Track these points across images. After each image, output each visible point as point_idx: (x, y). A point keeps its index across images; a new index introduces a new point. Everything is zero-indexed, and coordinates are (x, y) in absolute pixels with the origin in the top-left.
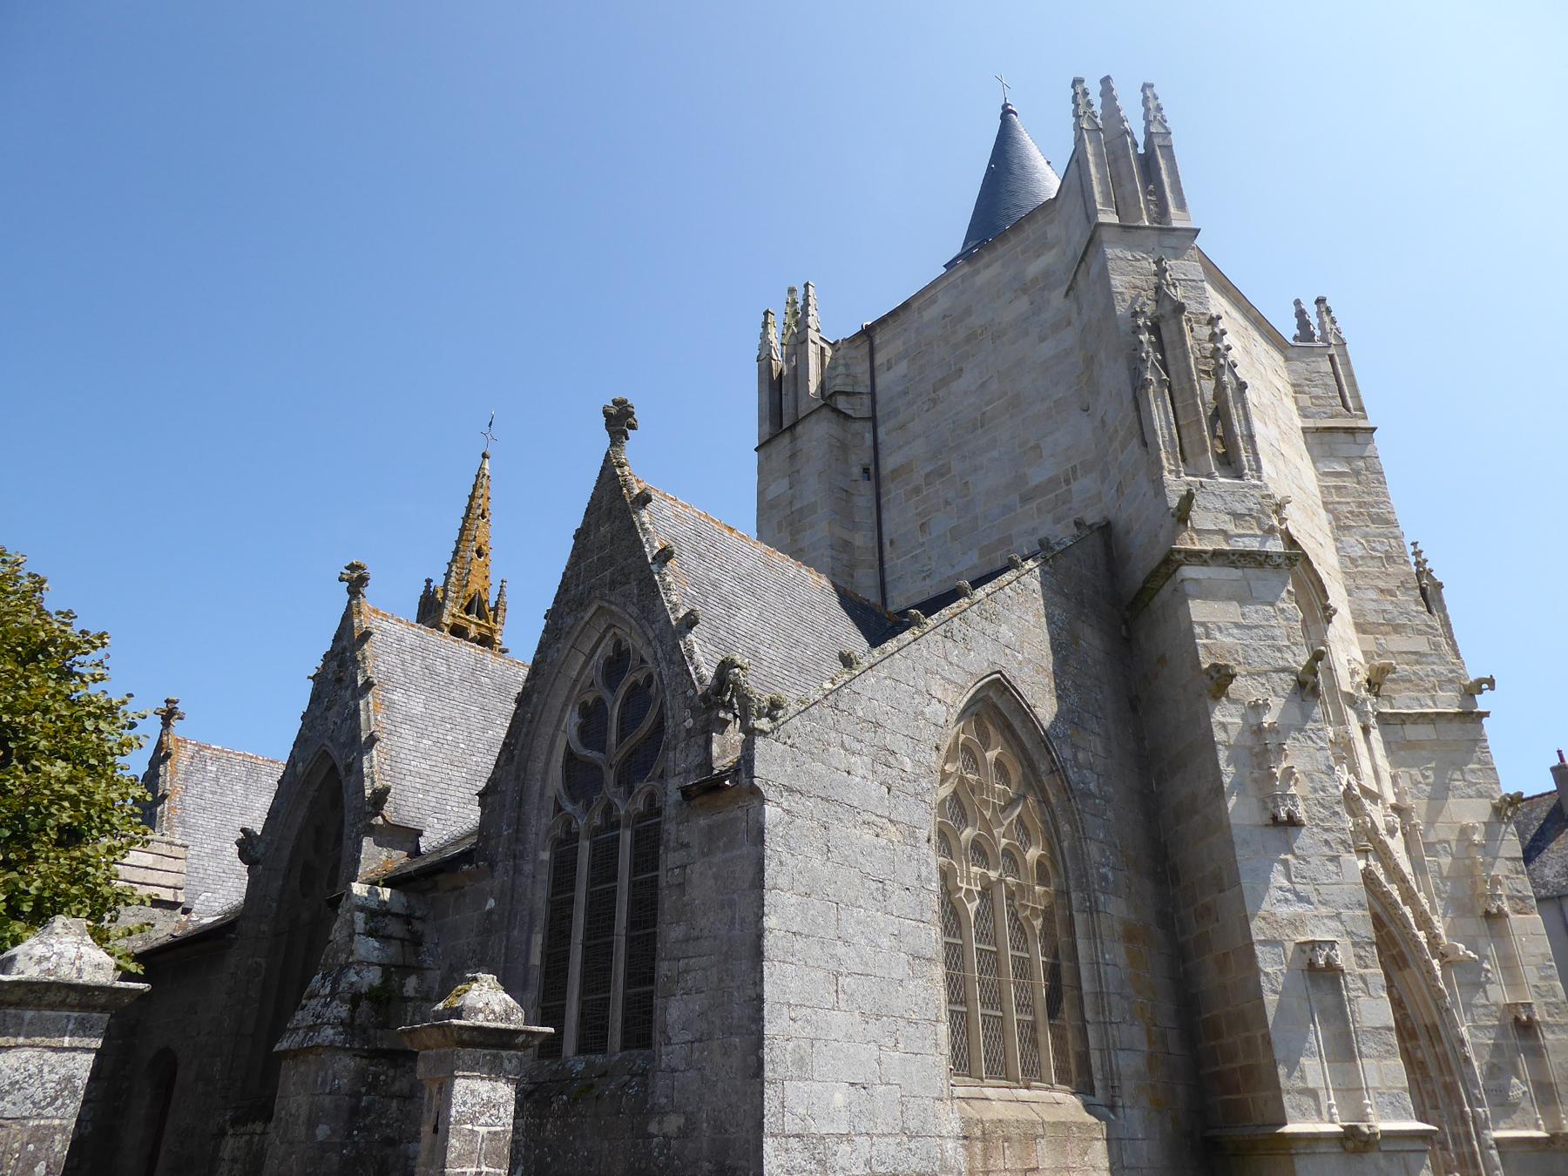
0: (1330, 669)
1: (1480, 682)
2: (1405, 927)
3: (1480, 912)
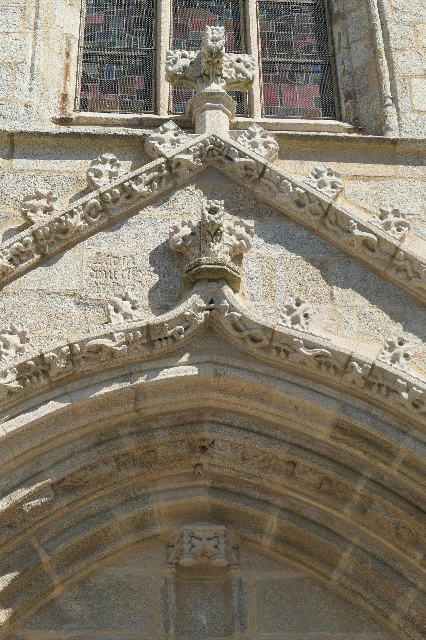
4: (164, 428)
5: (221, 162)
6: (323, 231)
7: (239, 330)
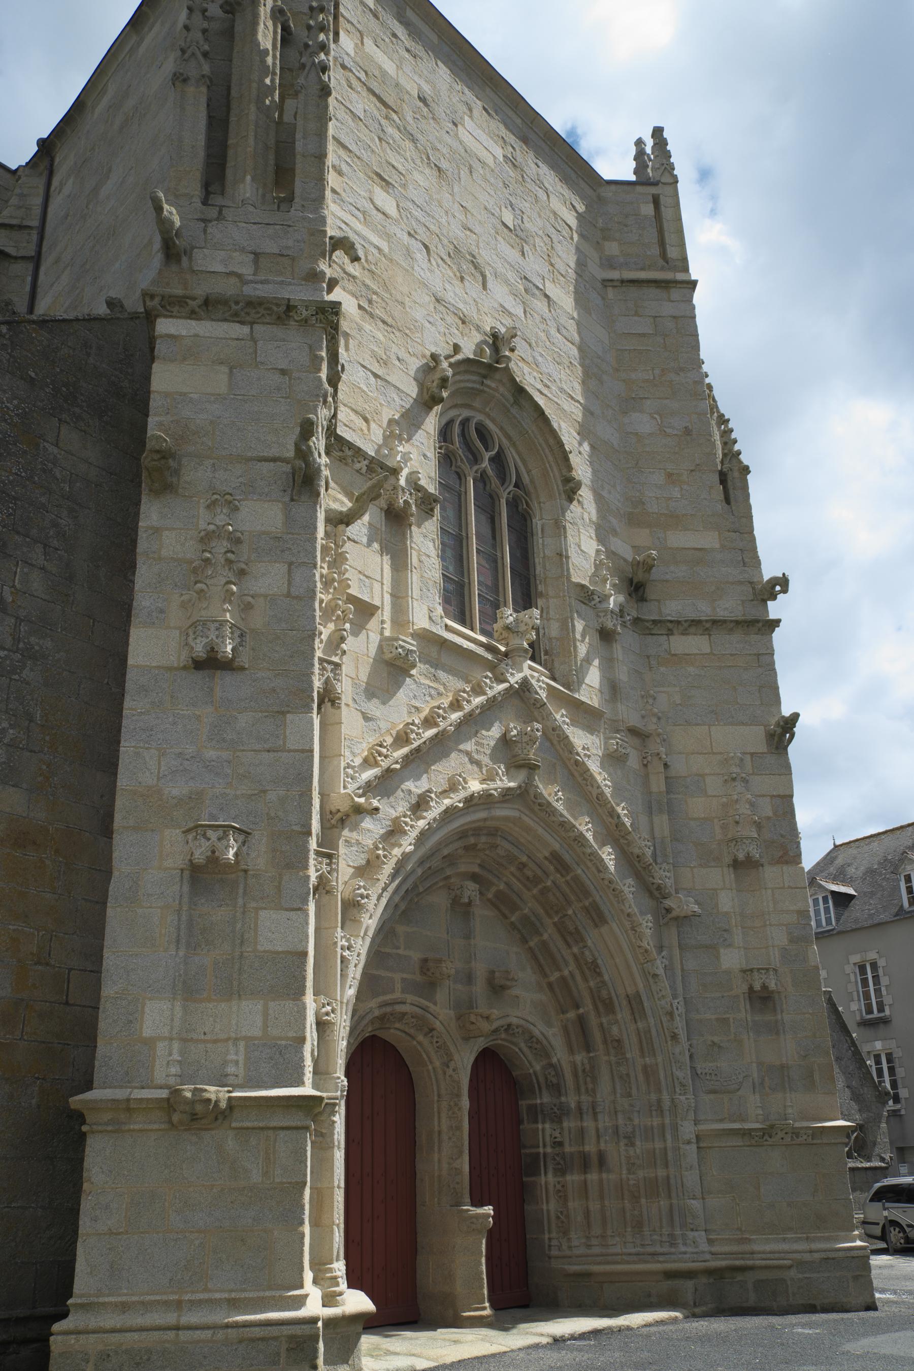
0: (561, 555)
1: (774, 581)
2: (599, 871)
3: (728, 860)
5: (524, 692)
6: (558, 747)
7: (536, 799)
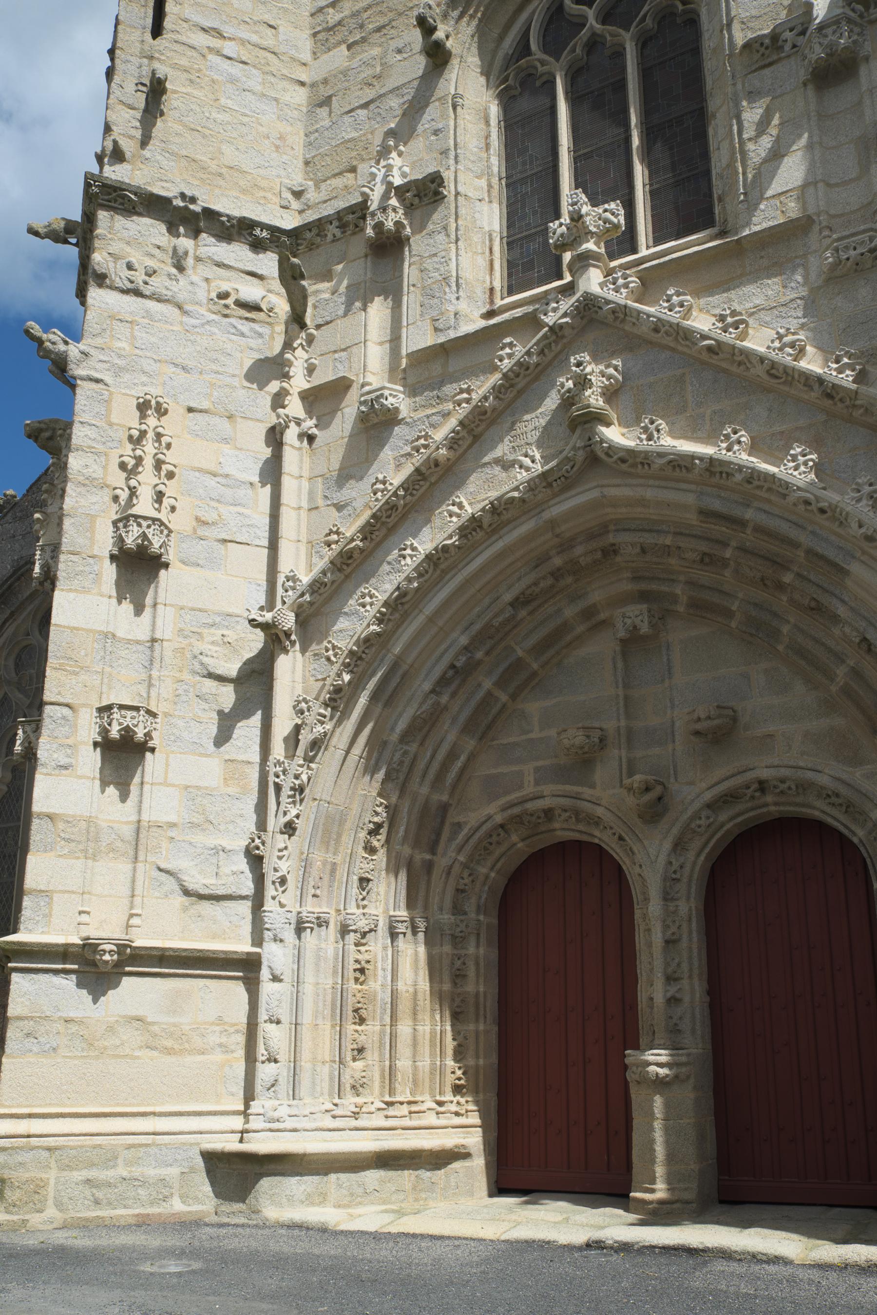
4: (581, 543)
